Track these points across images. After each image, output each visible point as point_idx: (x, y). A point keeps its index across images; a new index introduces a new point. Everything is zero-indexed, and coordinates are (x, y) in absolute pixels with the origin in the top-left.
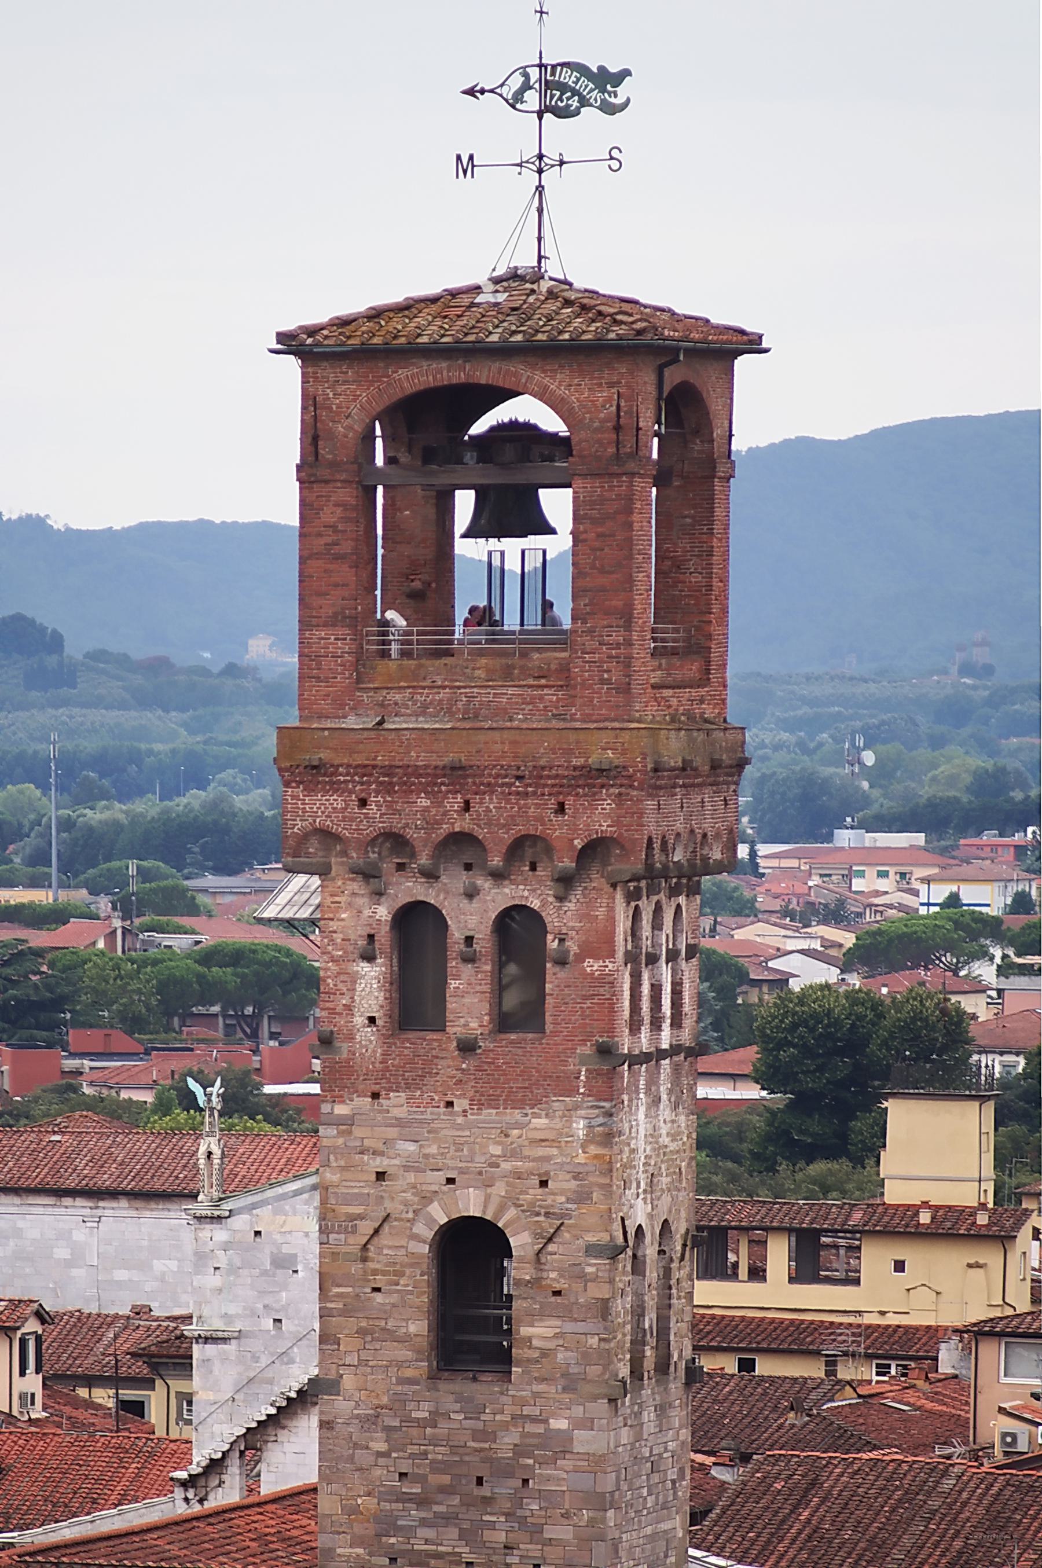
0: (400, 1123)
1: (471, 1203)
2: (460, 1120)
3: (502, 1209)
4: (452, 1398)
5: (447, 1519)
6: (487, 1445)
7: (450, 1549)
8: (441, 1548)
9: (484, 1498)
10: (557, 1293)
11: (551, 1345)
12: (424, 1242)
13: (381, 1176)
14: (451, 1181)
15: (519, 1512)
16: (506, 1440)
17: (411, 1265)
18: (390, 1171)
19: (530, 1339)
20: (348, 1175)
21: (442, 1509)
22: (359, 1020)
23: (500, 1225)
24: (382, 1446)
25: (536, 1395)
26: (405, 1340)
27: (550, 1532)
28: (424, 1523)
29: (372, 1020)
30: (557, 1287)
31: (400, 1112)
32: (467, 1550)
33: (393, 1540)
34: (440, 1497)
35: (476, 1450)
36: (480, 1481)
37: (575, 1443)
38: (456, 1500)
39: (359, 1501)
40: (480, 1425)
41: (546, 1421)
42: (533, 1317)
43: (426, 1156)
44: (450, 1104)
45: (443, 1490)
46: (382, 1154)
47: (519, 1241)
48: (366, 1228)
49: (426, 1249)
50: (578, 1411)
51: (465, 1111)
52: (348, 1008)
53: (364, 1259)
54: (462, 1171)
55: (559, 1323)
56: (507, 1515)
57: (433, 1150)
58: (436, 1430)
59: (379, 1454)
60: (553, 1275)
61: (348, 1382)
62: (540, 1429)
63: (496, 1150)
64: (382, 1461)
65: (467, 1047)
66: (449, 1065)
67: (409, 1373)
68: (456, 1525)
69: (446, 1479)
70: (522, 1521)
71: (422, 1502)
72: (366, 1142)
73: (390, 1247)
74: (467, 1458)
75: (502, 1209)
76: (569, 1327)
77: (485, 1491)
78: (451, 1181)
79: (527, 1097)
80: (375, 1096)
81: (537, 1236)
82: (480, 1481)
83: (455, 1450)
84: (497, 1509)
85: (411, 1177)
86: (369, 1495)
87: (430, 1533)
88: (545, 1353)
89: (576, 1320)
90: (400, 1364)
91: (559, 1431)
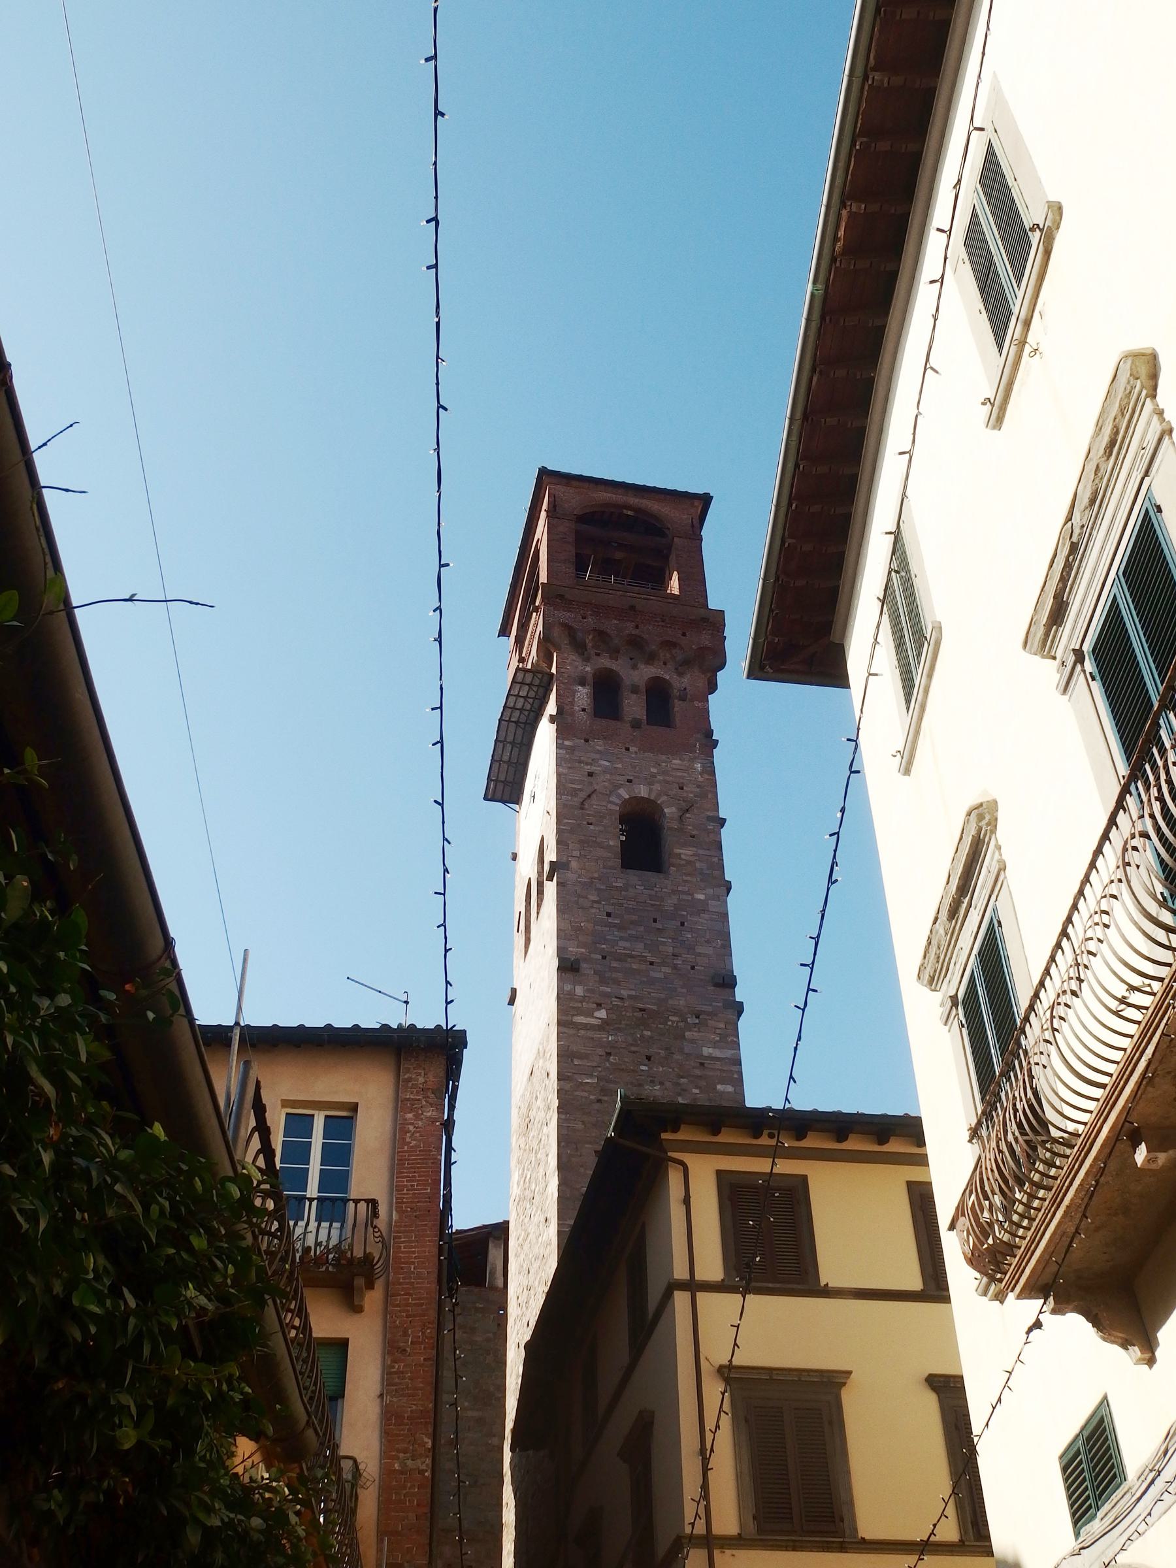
0: (599, 752)
1: (643, 791)
3: (659, 795)
10: (693, 837)
11: (693, 859)
13: (590, 774)
14: (630, 781)
27: (699, 949)
28: (622, 938)
29: (584, 710)
36: (655, 921)
38: (642, 929)
40: (653, 893)
41: (692, 895)
44: (627, 749)
45: (632, 922)
46: (591, 764)
48: (583, 795)
52: (572, 703)
53: (582, 809)
57: (620, 766)
59: (593, 901)
61: (574, 864)
62: (690, 898)
63: (653, 770)
64: (595, 905)
65: (636, 725)
67: (610, 864)
69: (635, 918)
71: (620, 928)
76: (701, 852)
77: (659, 925)
78: (630, 781)
80: (587, 741)
81: (679, 809)
82: (655, 921)
85: (608, 776)
87: (627, 944)
88: (689, 862)
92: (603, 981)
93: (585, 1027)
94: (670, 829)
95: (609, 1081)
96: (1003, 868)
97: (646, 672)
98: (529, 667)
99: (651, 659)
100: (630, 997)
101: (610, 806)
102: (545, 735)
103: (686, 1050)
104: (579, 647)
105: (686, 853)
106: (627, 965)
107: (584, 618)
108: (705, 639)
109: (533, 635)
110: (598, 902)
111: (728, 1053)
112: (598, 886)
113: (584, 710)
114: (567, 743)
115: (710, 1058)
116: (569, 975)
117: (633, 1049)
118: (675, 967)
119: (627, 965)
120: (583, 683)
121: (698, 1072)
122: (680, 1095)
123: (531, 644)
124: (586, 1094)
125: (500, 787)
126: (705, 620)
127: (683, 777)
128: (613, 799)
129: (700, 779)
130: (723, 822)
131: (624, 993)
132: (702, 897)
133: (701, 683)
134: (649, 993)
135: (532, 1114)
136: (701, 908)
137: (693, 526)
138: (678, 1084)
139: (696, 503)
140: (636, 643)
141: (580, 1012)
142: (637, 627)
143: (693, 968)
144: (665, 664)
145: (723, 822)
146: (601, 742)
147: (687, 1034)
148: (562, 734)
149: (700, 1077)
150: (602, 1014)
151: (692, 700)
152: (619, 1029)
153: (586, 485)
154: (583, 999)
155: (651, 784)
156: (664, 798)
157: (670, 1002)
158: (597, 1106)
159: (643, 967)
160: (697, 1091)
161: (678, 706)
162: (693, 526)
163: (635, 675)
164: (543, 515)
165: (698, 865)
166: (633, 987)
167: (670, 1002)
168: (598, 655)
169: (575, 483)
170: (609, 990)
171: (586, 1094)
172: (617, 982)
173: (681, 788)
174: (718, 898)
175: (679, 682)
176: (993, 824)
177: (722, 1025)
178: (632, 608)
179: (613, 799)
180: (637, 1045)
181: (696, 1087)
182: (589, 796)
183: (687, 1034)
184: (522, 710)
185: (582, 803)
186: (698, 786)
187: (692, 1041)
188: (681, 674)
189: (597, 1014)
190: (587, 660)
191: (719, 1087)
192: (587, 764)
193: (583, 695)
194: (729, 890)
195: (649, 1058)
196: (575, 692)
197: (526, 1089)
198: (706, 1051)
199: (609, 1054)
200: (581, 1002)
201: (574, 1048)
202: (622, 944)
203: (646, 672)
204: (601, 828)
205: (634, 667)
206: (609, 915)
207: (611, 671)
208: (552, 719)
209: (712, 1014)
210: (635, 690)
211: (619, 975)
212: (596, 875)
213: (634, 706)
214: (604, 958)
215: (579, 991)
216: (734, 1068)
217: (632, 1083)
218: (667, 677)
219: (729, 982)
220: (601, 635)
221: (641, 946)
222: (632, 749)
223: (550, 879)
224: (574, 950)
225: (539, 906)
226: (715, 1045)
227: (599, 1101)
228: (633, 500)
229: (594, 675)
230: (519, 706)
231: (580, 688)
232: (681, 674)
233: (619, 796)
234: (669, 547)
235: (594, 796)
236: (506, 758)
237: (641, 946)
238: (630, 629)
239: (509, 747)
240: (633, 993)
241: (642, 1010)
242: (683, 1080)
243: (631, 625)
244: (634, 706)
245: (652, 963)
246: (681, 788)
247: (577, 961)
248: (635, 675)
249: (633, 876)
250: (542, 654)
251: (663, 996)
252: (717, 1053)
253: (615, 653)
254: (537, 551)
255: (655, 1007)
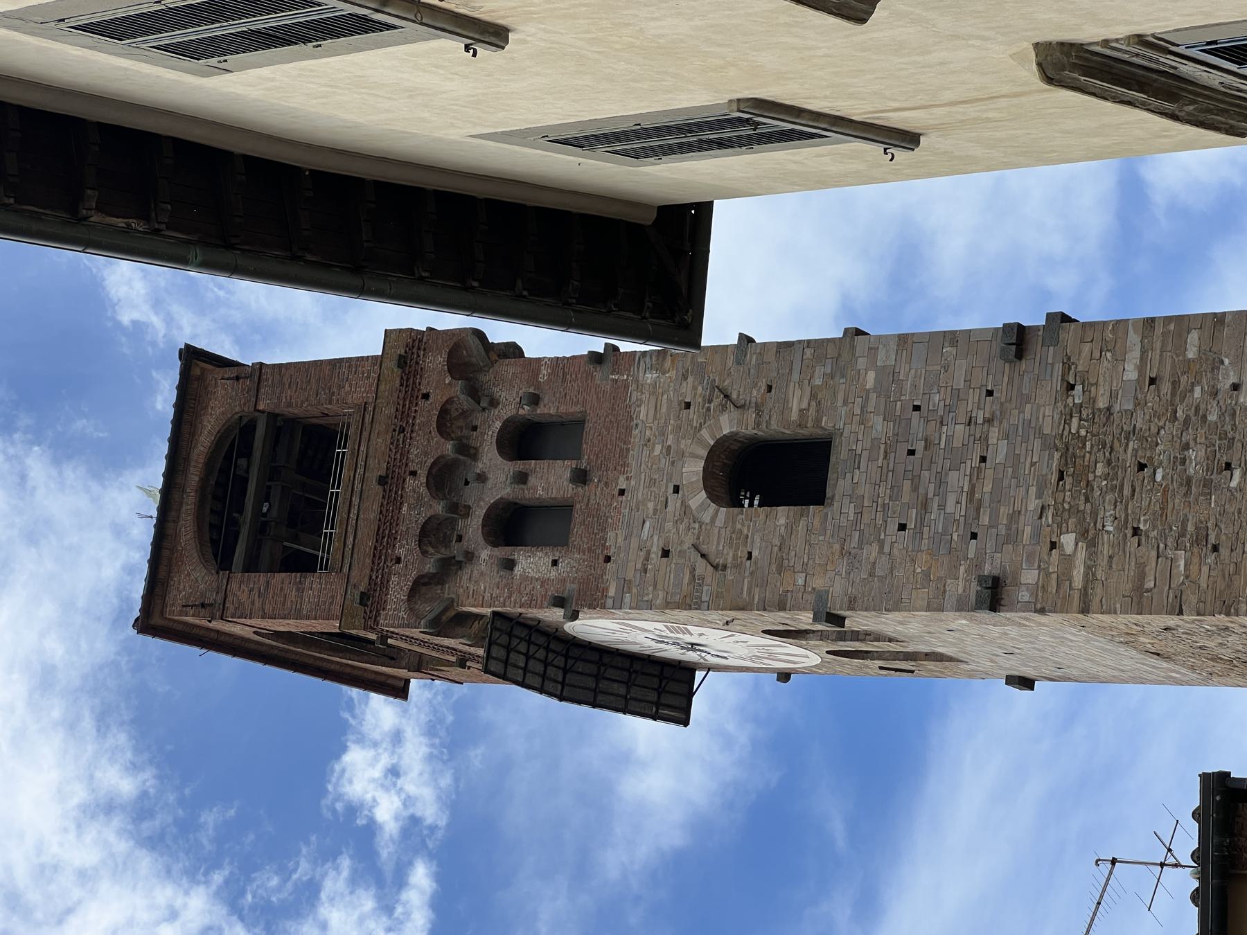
0: (628, 537)
1: (693, 469)
2: (633, 483)
3: (701, 442)
4: (841, 482)
5: (941, 482)
6: (883, 447)
7: (967, 478)
8: (966, 489)
9: (925, 448)
10: (770, 388)
12: (717, 512)
13: (666, 553)
14: (676, 489)
15: (941, 413)
16: (879, 428)
17: (734, 523)
18: (661, 545)
19: (801, 411)
20: (660, 586)
21: (932, 487)
22: (553, 574)
23: (712, 443)
24: (875, 548)
25: (845, 402)
26: (791, 527)
28: (942, 506)
29: (555, 563)
30: (764, 388)
31: (621, 534)
32: (969, 462)
33: (955, 537)
34: (921, 491)
35: (885, 458)
37: (888, 363)
39: (919, 570)
40: (865, 454)
41: (868, 391)
42: (785, 407)
43: (655, 511)
44: (622, 492)
45: (915, 488)
46: (649, 552)
47: (727, 424)
48: (702, 567)
49: (723, 510)
50: (862, 363)
51: (627, 479)
52: (544, 583)
53: (725, 567)
54: (669, 479)
55: (792, 385)
56: (942, 424)
57: (651, 505)
58: (866, 496)
59: (881, 551)
60: (755, 392)
61: (818, 583)
62: (873, 396)
63: (658, 449)
64: (887, 549)
65: (581, 477)
66: (594, 492)
67: (817, 523)
68: (947, 474)
69: (907, 485)
70: (949, 409)
71: (925, 507)
72: (639, 566)
73: (718, 543)
74: (891, 467)
75: (701, 442)
76: (795, 376)
77: (919, 447)
78: (676, 489)
79: (623, 422)
80: (608, 559)
81: (724, 409)
82: (911, 452)
83: (884, 478)
84: (937, 435)
85: (669, 525)
86: (913, 560)
88: (813, 396)
89: (791, 370)
90: (809, 532)
91: (876, 379)
92: (1011, 538)
93: (1089, 569)
94: (757, 424)
95: (1182, 534)
96: (1140, 40)
97: (492, 462)
98: (481, 652)
99: (468, 451)
100: (1039, 495)
101: (720, 522)
102: (595, 627)
103: (1131, 407)
104: (449, 567)
105: (797, 401)
106: (987, 497)
107: (398, 560)
108: (436, 362)
109: (423, 643)
110: (881, 544)
111: (1134, 338)
112: (854, 543)
113: (555, 563)
114: (612, 592)
115: (1141, 369)
116: (1008, 593)
117: (1127, 492)
118: (989, 421)
119: (987, 497)
120: (509, 565)
121: (1166, 387)
122: (1204, 417)
123: (436, 647)
124: (1205, 569)
125: (666, 699)
126: (402, 362)
127: (669, 401)
128: (706, 518)
129: (672, 374)
130: (746, 340)
131: (1034, 504)
132: (871, 376)
133: (508, 368)
134: (1033, 464)
135: (1227, 654)
136: (889, 376)
137: (237, 378)
138: (1187, 421)
139: (196, 371)
140: (444, 478)
141: (1065, 576)
142: (414, 473)
143: (990, 393)
144: (475, 428)
145: (746, 340)
146: (611, 535)
147: (1102, 404)
148: (596, 601)
149: (1175, 384)
150: (1068, 540)
151: (538, 385)
152: (1094, 514)
153: (166, 553)
154: (1044, 571)
155: (683, 455)
156: (705, 433)
157: (1047, 431)
158: (1224, 552)
159: (989, 473)
160: (1198, 390)
161: (549, 409)
162: (237, 378)
163: (496, 478)
164: (216, 625)
165: (818, 381)
166: (1022, 491)
167: (1047, 431)
168: (460, 539)
169: (162, 574)
170: (1028, 530)
171: (1205, 569)
172: (1015, 516)
173: (688, 405)
174: (873, 351)
175: (510, 404)
176: (1068, 48)
177: (1086, 348)
178: (382, 481)
179: (706, 518)
180: (1122, 486)
181: (1192, 391)
182: (703, 556)
183: (1102, 404)
184: (546, 664)
185: (716, 567)
186: (685, 377)
187: (1113, 395)
188: (494, 403)
189: (1069, 549)
190: (470, 556)
191: (1191, 355)
192: (647, 559)
193: (533, 564)
194: (859, 332)
195: (1142, 467)
196: (525, 578)
197: (1184, 664)
198: (1131, 374)
199: (1136, 532)
200: (1048, 574)
201: (1126, 587)
202: (950, 508)
203: (492, 462)
204: (757, 538)
205: (482, 478)
206: (902, 527)
207: (487, 517)
208: (574, 616)
209: (1067, 364)
210: (522, 478)
211: (1004, 511)
212: (837, 547)
213: (549, 480)
214: (974, 536)
215: (1030, 576)
216: (1159, 330)
217: (1186, 495)
218: (498, 424)
219: (1018, 340)
220: (431, 533)
221: (953, 476)
222: (622, 484)
223: (838, 620)
224: (962, 584)
225: (878, 637)
226: (1120, 359)
227: (1215, 548)
228: (194, 477)
229: (495, 544)
230: (539, 668)
231: (518, 569)
232: (494, 403)
233: (702, 507)
234: (272, 416)
235: (704, 548)
236: (622, 690)
237: (953, 476)
238: (416, 486)
239: (603, 685)
240: (1033, 490)
241: (1061, 478)
242: (1179, 414)
243: (410, 483)
244: (549, 480)
245: (983, 459)
246: (688, 405)
247: (981, 580)
248: (496, 478)
249: (839, 485)
250: (459, 630)
251: (1038, 443)
252: (1134, 356)
253: (459, 510)
254: (277, 635)
255: (1057, 455)
